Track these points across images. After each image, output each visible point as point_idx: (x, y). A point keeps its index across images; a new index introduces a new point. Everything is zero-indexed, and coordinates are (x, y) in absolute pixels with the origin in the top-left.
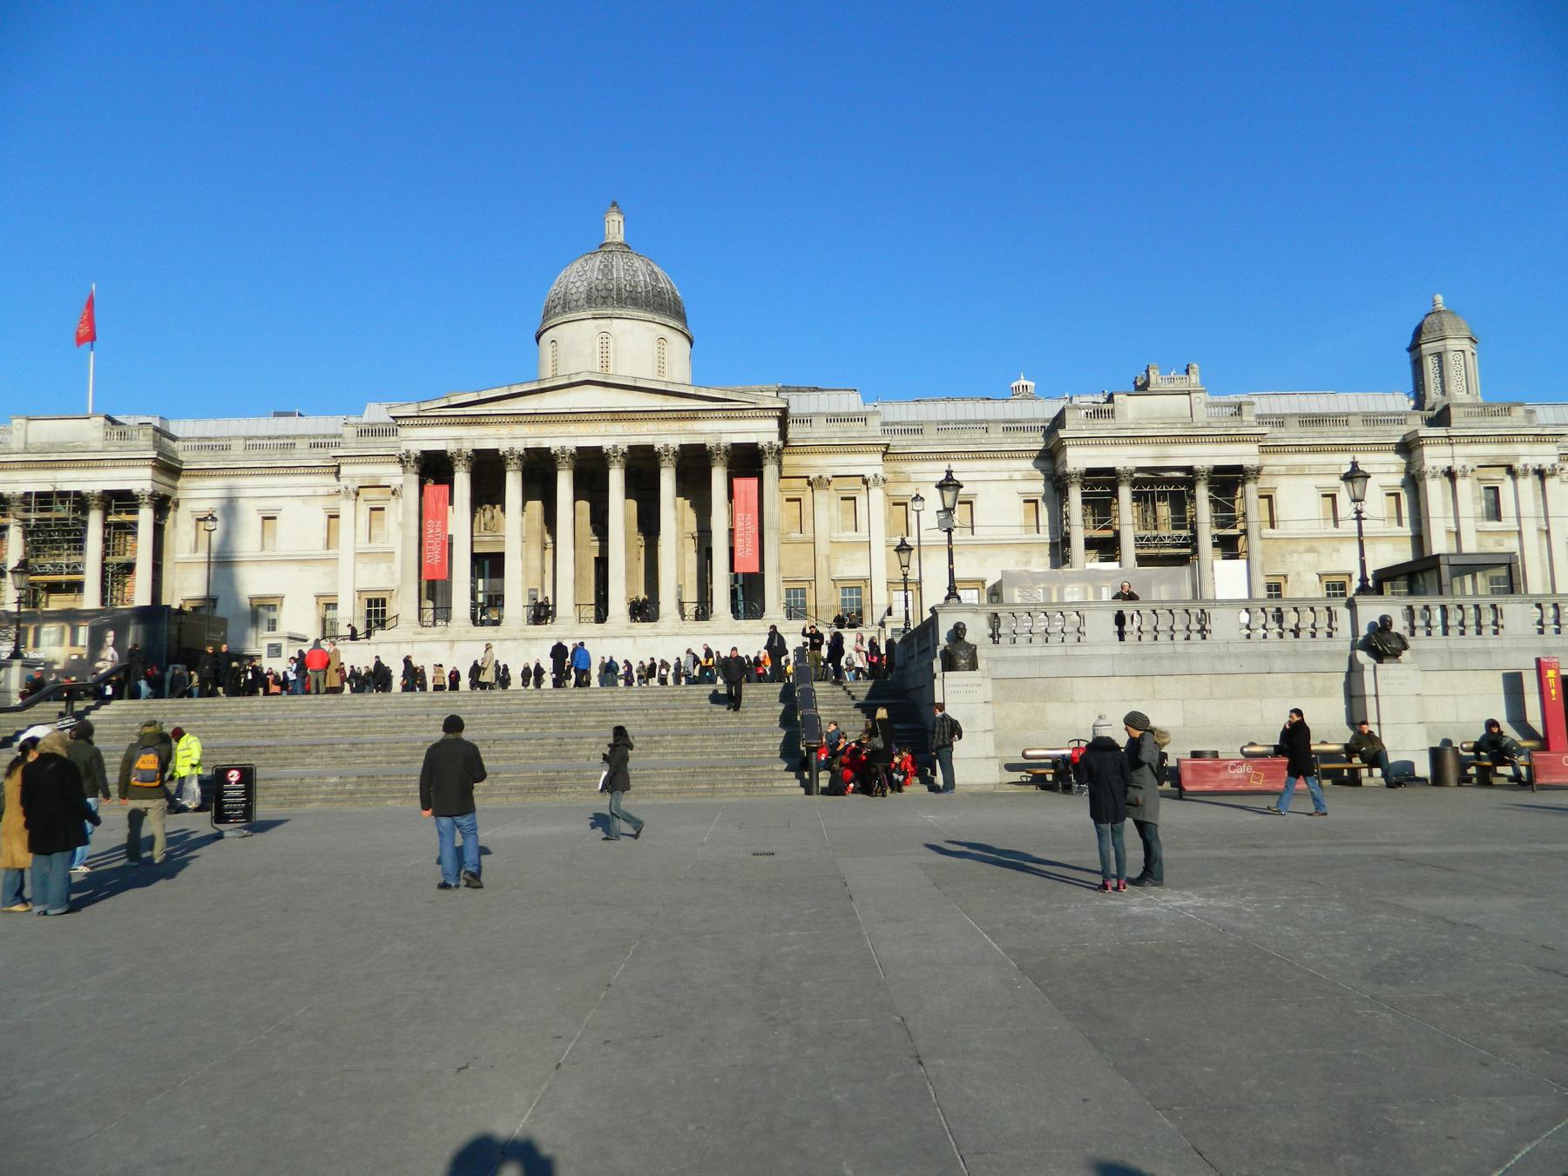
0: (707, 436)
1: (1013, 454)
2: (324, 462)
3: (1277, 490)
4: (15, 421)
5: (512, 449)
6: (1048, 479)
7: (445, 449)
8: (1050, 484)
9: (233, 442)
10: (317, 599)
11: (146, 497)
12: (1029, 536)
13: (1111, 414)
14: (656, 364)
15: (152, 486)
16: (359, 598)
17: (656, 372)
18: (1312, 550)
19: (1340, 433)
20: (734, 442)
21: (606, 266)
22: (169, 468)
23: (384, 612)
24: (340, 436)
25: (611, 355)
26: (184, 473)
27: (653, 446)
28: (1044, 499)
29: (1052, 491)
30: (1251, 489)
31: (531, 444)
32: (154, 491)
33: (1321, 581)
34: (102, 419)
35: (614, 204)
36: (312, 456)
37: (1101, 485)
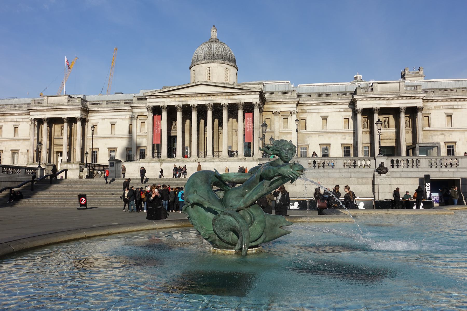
1: (340, 103)
3: (431, 115)
8: (353, 113)
9: (103, 102)
12: (345, 130)
13: (372, 89)
14: (225, 77)
17: (225, 79)
18: (442, 134)
19: (453, 95)
22: (86, 111)
23: (145, 153)
24: (132, 100)
25: (211, 75)
26: (90, 112)
27: (220, 104)
28: (352, 118)
29: (354, 115)
30: (419, 114)
31: (185, 103)
32: (81, 117)
33: (445, 145)
34: (67, 96)
35: (214, 26)
37: (368, 112)
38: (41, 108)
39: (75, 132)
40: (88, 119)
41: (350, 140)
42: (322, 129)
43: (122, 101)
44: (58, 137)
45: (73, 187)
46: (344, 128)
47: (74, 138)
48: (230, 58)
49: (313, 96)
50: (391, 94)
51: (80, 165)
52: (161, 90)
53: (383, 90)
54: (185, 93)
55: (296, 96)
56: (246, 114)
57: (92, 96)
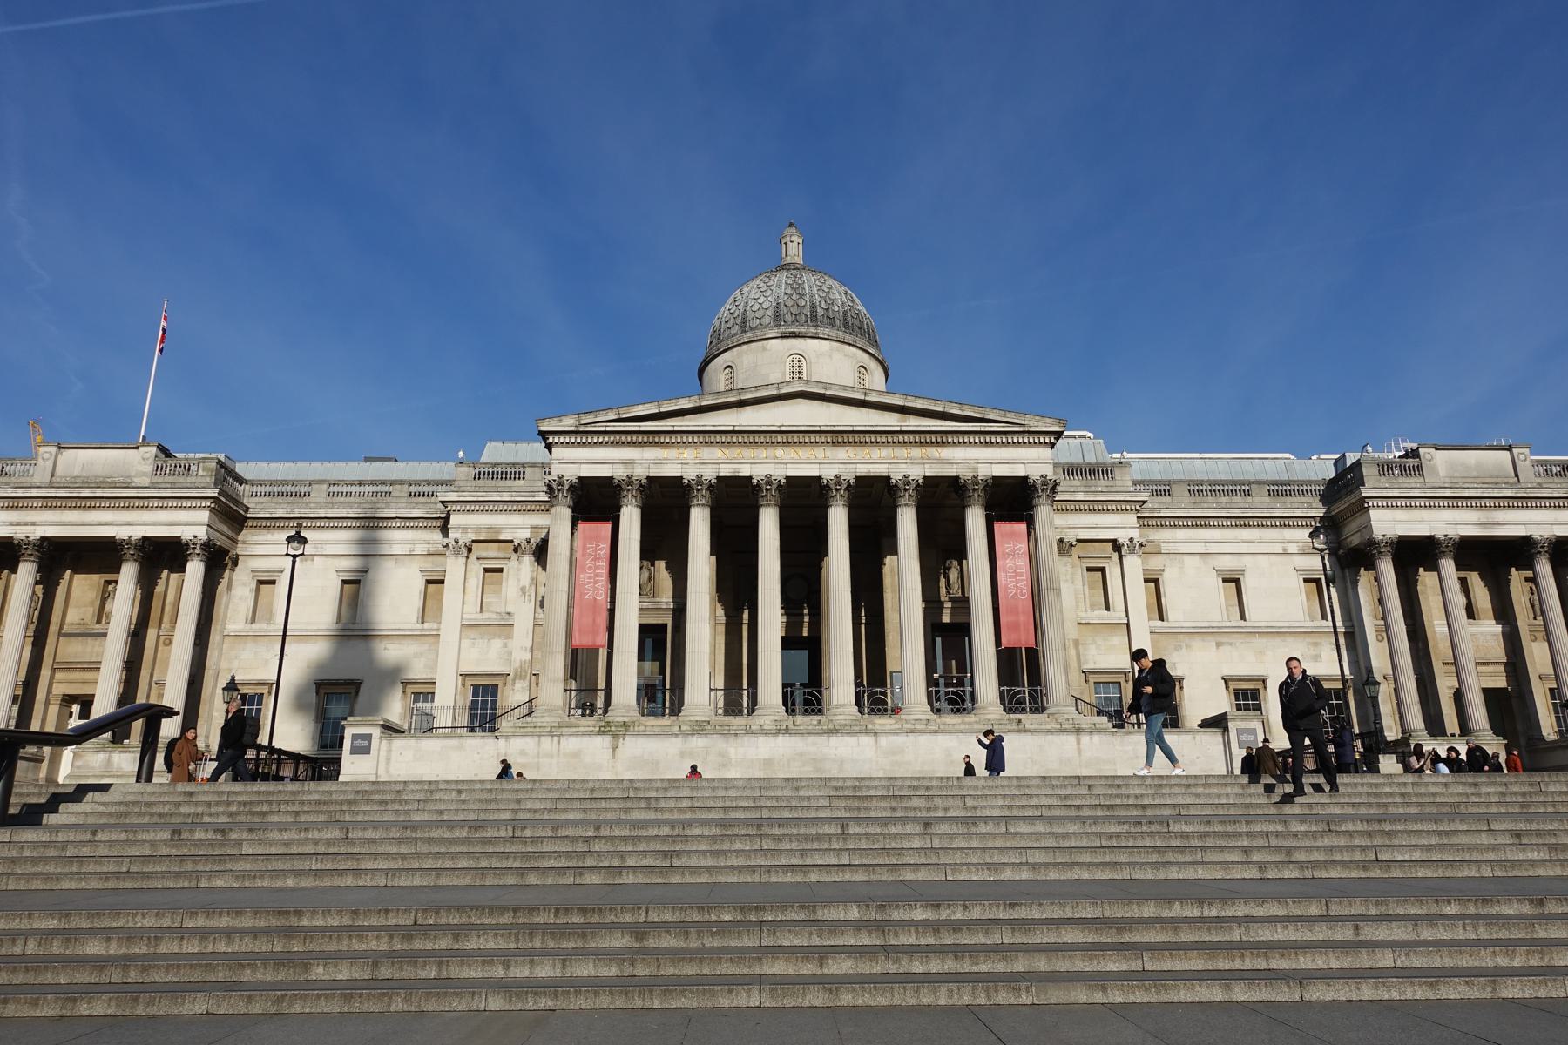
1: (1285, 523)
4: (42, 449)
6: (1333, 553)
7: (610, 475)
10: (404, 688)
11: (198, 547)
13: (1419, 470)
15: (207, 533)
16: (463, 685)
22: (231, 515)
23: (494, 702)
26: (249, 523)
31: (726, 471)
32: (209, 540)
34: (154, 450)
35: (791, 225)
36: (411, 506)
38: (20, 493)
39: (168, 608)
40: (238, 555)
43: (398, 487)
45: (246, 850)
46: (1308, 618)
47: (158, 636)
48: (869, 331)
49: (1180, 492)
50: (1491, 486)
52: (621, 410)
53: (1456, 474)
54: (731, 428)
55: (1130, 483)
56: (998, 527)
57: (264, 464)
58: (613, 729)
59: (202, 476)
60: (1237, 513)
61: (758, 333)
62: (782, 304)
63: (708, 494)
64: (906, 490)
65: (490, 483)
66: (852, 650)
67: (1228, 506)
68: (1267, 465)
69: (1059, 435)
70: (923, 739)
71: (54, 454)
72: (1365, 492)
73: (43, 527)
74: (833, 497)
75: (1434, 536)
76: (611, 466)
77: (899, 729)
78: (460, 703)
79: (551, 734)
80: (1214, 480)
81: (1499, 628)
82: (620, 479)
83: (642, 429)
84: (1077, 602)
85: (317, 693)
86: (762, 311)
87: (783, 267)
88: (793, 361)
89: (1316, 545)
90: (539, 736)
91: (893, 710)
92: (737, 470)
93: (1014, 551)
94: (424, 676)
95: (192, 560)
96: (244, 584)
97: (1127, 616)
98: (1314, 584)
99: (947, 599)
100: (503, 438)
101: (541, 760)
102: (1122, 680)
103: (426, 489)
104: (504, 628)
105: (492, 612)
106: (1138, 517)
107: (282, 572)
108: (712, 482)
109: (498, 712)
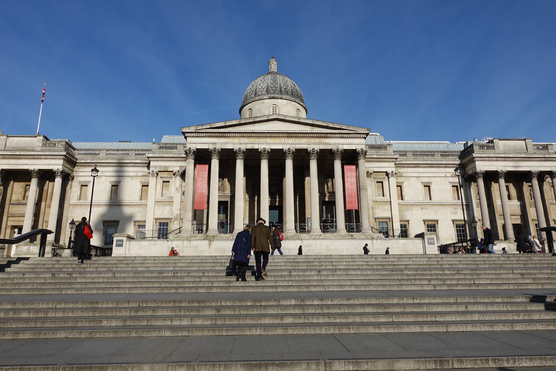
0: (332, 145)
1: (446, 166)
2: (142, 161)
5: (240, 149)
7: (208, 148)
9: (101, 151)
10: (135, 223)
12: (456, 201)
16: (156, 222)
20: (345, 148)
21: (274, 78)
22: (71, 161)
26: (78, 164)
31: (249, 147)
32: (63, 170)
34: (42, 137)
35: (273, 57)
39: (49, 195)
40: (74, 176)
41: (460, 215)
42: (424, 199)
43: (131, 152)
44: (18, 201)
45: (78, 280)
46: (453, 199)
47: (46, 205)
49: (410, 155)
51: (53, 248)
52: (212, 125)
53: (506, 149)
54: (251, 131)
55: (392, 152)
56: (345, 167)
57: (82, 143)
58: (209, 238)
59: (60, 147)
60: (429, 162)
61: (261, 97)
62: (269, 86)
63: (243, 155)
64: (313, 154)
65: (165, 150)
66: (294, 210)
67: (426, 160)
68: (441, 146)
69: (367, 134)
70: (318, 241)
71: (5, 139)
72: (474, 155)
73: (2, 165)
74: (287, 156)
75: (497, 171)
76: (208, 144)
77: (310, 238)
78: (155, 229)
79: (187, 240)
80: (422, 151)
81: (519, 203)
82: (211, 149)
83: (219, 131)
84: (373, 194)
85: (104, 225)
86: (262, 89)
87: (270, 73)
88: (273, 107)
89: (457, 174)
90: (183, 240)
91: (308, 231)
92: (253, 146)
93: (351, 176)
94: (142, 219)
95: (57, 178)
96: (76, 186)
97: (390, 199)
98: (456, 188)
99: (327, 192)
100: (169, 134)
101: (184, 249)
102: (388, 221)
103: (142, 152)
104: (170, 202)
105: (166, 197)
106: (395, 164)
107: (90, 182)
108: (244, 150)
109: (168, 232)
